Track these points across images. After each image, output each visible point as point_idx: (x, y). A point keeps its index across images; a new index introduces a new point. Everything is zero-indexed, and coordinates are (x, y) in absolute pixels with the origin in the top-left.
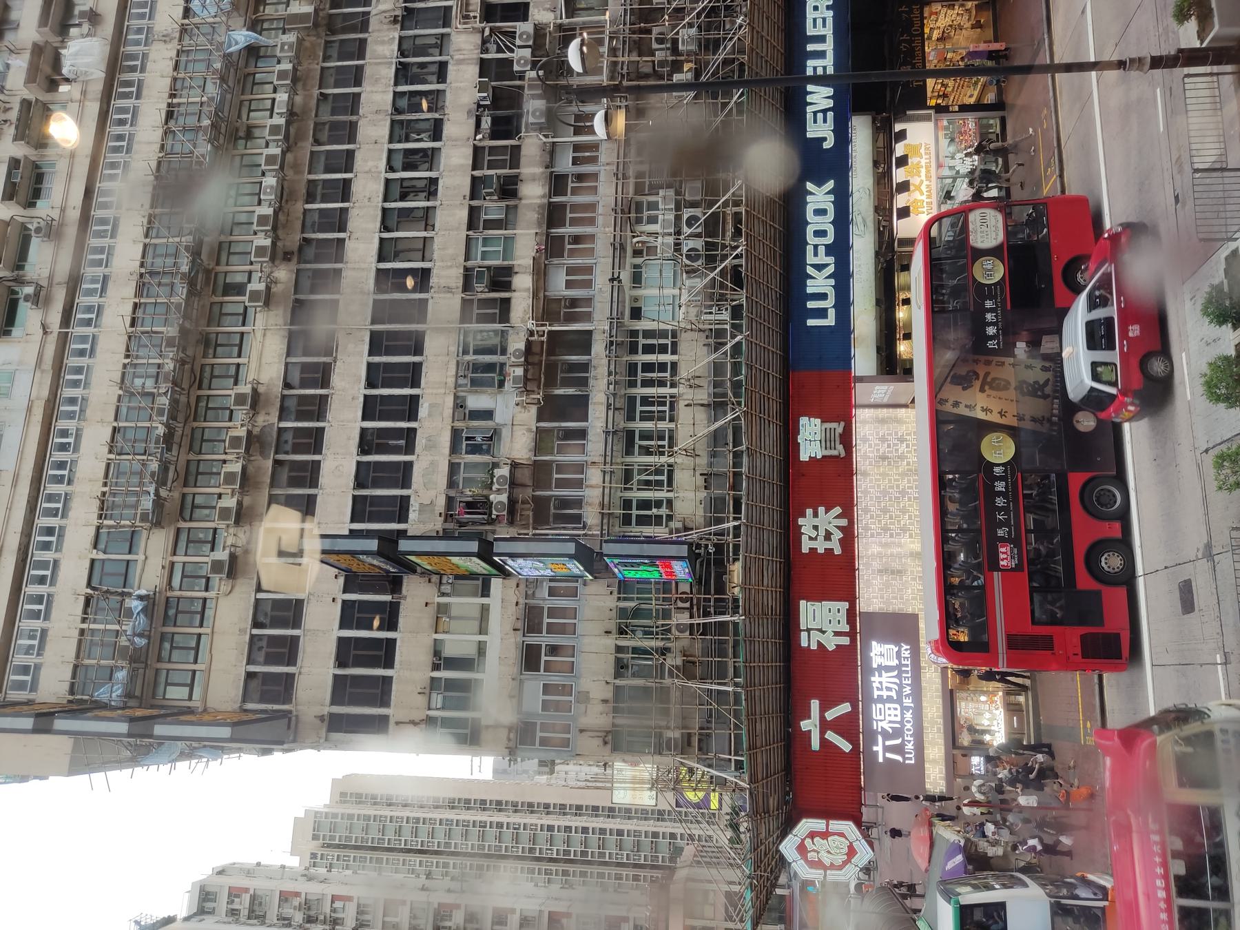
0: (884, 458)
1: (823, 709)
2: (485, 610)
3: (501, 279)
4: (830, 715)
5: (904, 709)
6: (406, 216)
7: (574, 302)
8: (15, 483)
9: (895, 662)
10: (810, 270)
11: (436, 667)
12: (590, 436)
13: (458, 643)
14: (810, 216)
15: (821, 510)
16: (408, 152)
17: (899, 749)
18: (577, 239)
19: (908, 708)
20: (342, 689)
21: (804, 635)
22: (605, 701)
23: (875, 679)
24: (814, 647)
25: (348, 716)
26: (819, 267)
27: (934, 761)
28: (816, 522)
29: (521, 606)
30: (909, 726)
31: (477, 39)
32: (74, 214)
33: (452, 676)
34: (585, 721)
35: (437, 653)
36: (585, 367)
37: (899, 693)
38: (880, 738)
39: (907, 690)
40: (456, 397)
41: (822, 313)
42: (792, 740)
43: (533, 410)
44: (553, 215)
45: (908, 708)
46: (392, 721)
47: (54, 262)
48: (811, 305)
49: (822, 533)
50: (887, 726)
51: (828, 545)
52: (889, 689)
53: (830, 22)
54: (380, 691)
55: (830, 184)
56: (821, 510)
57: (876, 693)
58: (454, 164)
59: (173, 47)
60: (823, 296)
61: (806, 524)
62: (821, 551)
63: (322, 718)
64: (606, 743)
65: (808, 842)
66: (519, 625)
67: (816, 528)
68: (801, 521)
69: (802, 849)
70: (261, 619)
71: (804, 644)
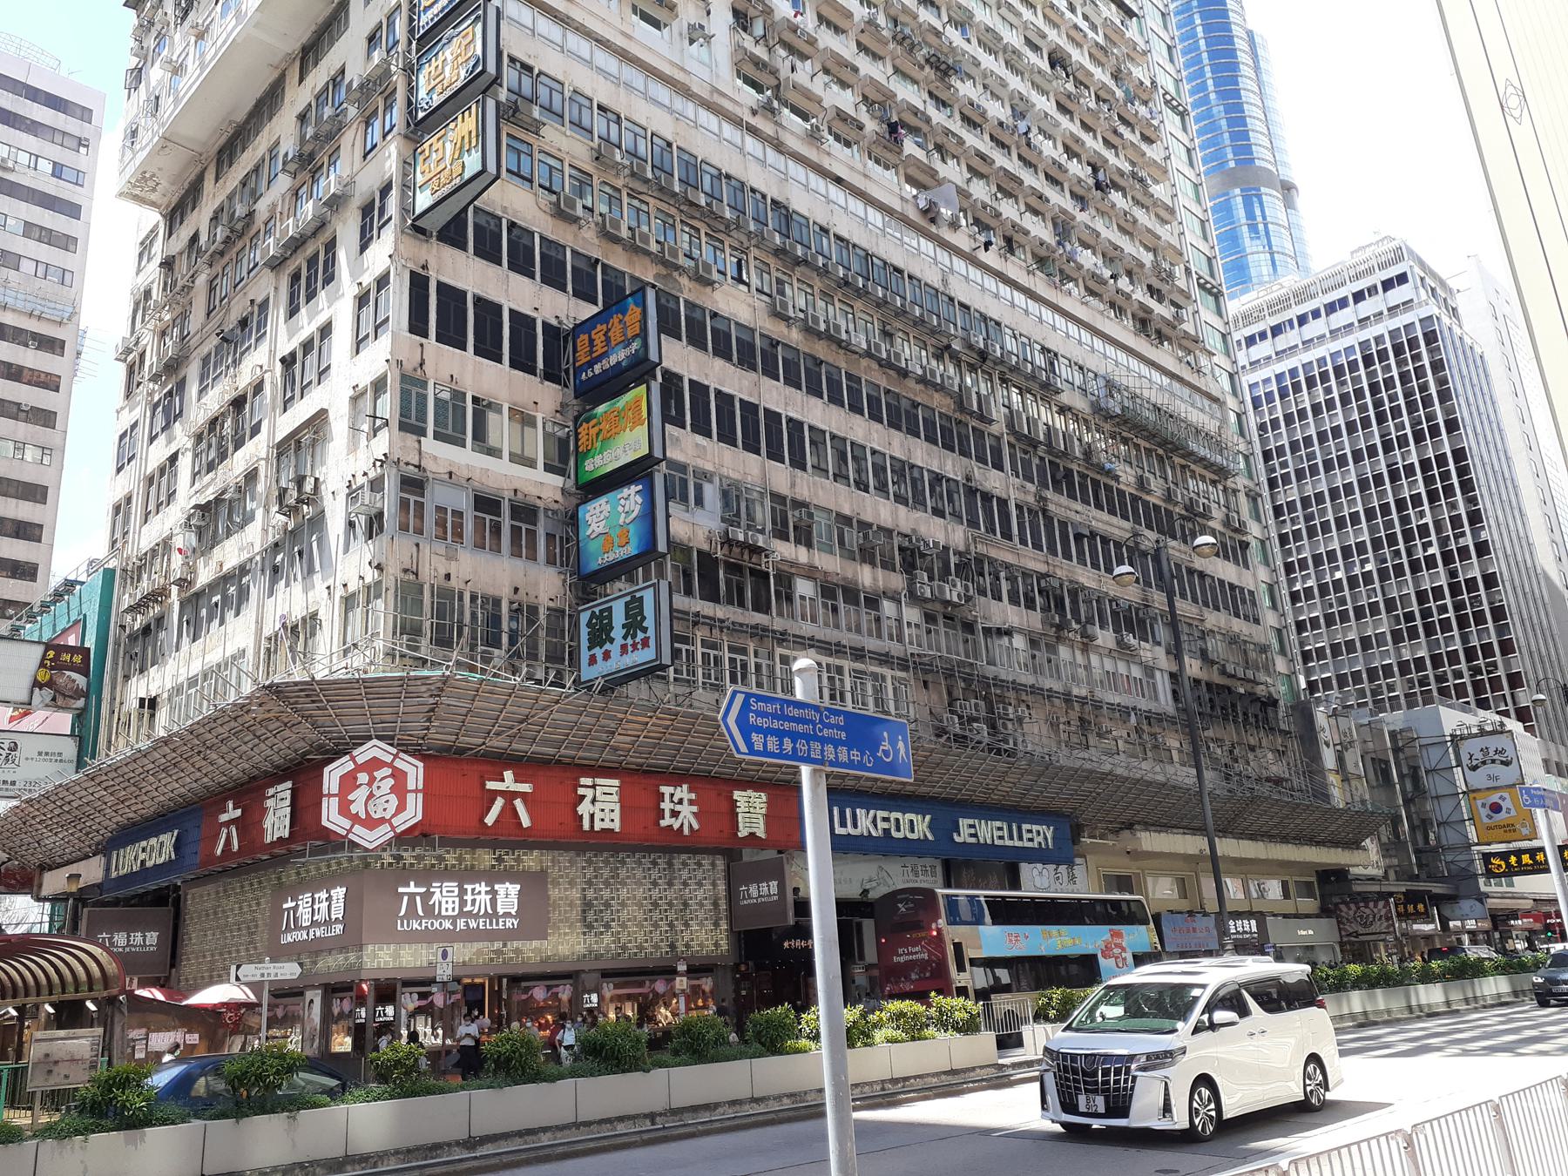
0: (686, 904)
1: (523, 795)
2: (531, 464)
3: (804, 537)
4: (518, 803)
5: (454, 919)
6: (842, 457)
7: (790, 599)
8: (624, 34)
9: (501, 911)
10: (872, 812)
11: (475, 400)
12: (686, 600)
13: (500, 429)
14: (909, 816)
15: (695, 809)
16: (884, 469)
17: (412, 913)
18: (835, 609)
19: (454, 924)
20: (452, 297)
21: (589, 781)
22: (448, 577)
23: (483, 888)
24: (581, 791)
25: (427, 297)
26: (874, 822)
27: (396, 956)
28: (685, 802)
29: (538, 502)
30: (436, 925)
31: (962, 548)
32: (826, 163)
33: (464, 419)
34: (426, 549)
35: (490, 405)
36: (742, 604)
37: (469, 914)
38: (423, 890)
39: (473, 924)
40: (712, 474)
41: (843, 824)
42: (499, 761)
43: (706, 547)
44: (851, 593)
45: (454, 924)
46: (424, 340)
47: (792, 133)
48: (848, 811)
49: (678, 808)
50: (436, 897)
51: (667, 814)
52: (474, 901)
53: (1030, 845)
54: (451, 335)
55: (930, 837)
56: (695, 809)
57: (469, 887)
58: (881, 511)
59: (937, 284)
60: (855, 826)
61: (683, 792)
62: (663, 806)
63: (424, 267)
64: (406, 571)
65: (387, 771)
66: (520, 496)
67: (680, 802)
68: (685, 787)
69: (375, 764)
70: (515, 231)
71: (583, 781)
